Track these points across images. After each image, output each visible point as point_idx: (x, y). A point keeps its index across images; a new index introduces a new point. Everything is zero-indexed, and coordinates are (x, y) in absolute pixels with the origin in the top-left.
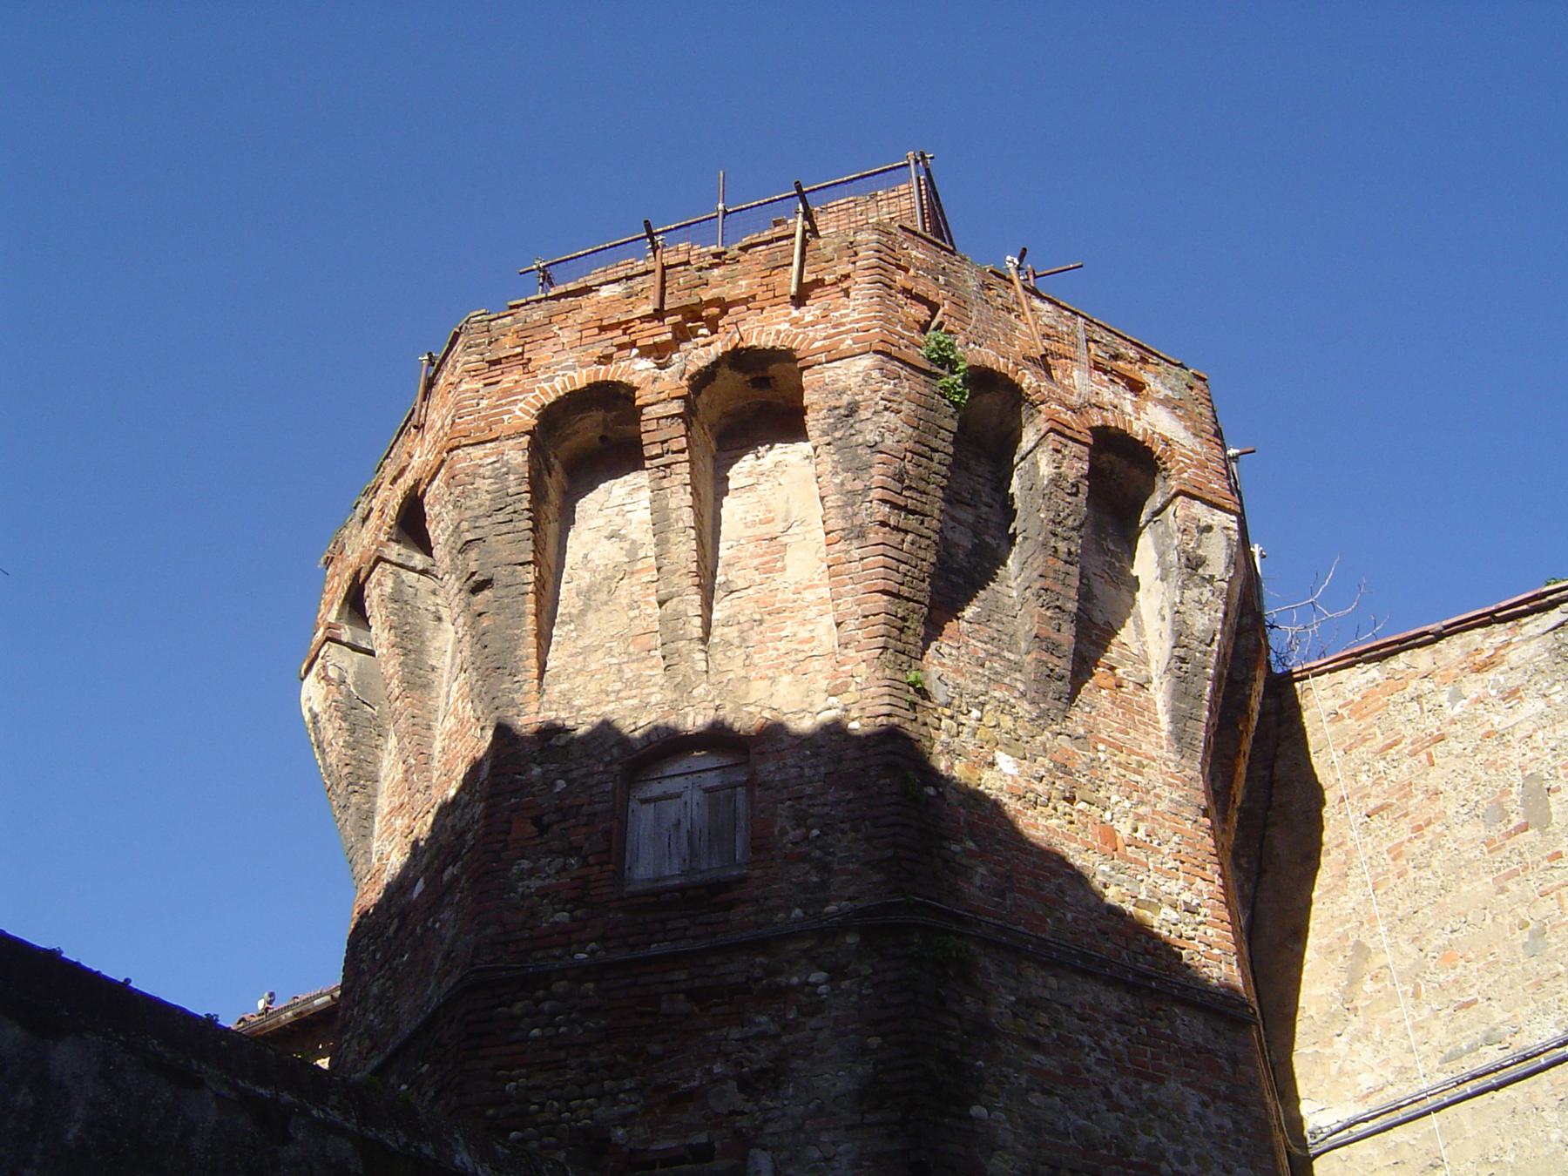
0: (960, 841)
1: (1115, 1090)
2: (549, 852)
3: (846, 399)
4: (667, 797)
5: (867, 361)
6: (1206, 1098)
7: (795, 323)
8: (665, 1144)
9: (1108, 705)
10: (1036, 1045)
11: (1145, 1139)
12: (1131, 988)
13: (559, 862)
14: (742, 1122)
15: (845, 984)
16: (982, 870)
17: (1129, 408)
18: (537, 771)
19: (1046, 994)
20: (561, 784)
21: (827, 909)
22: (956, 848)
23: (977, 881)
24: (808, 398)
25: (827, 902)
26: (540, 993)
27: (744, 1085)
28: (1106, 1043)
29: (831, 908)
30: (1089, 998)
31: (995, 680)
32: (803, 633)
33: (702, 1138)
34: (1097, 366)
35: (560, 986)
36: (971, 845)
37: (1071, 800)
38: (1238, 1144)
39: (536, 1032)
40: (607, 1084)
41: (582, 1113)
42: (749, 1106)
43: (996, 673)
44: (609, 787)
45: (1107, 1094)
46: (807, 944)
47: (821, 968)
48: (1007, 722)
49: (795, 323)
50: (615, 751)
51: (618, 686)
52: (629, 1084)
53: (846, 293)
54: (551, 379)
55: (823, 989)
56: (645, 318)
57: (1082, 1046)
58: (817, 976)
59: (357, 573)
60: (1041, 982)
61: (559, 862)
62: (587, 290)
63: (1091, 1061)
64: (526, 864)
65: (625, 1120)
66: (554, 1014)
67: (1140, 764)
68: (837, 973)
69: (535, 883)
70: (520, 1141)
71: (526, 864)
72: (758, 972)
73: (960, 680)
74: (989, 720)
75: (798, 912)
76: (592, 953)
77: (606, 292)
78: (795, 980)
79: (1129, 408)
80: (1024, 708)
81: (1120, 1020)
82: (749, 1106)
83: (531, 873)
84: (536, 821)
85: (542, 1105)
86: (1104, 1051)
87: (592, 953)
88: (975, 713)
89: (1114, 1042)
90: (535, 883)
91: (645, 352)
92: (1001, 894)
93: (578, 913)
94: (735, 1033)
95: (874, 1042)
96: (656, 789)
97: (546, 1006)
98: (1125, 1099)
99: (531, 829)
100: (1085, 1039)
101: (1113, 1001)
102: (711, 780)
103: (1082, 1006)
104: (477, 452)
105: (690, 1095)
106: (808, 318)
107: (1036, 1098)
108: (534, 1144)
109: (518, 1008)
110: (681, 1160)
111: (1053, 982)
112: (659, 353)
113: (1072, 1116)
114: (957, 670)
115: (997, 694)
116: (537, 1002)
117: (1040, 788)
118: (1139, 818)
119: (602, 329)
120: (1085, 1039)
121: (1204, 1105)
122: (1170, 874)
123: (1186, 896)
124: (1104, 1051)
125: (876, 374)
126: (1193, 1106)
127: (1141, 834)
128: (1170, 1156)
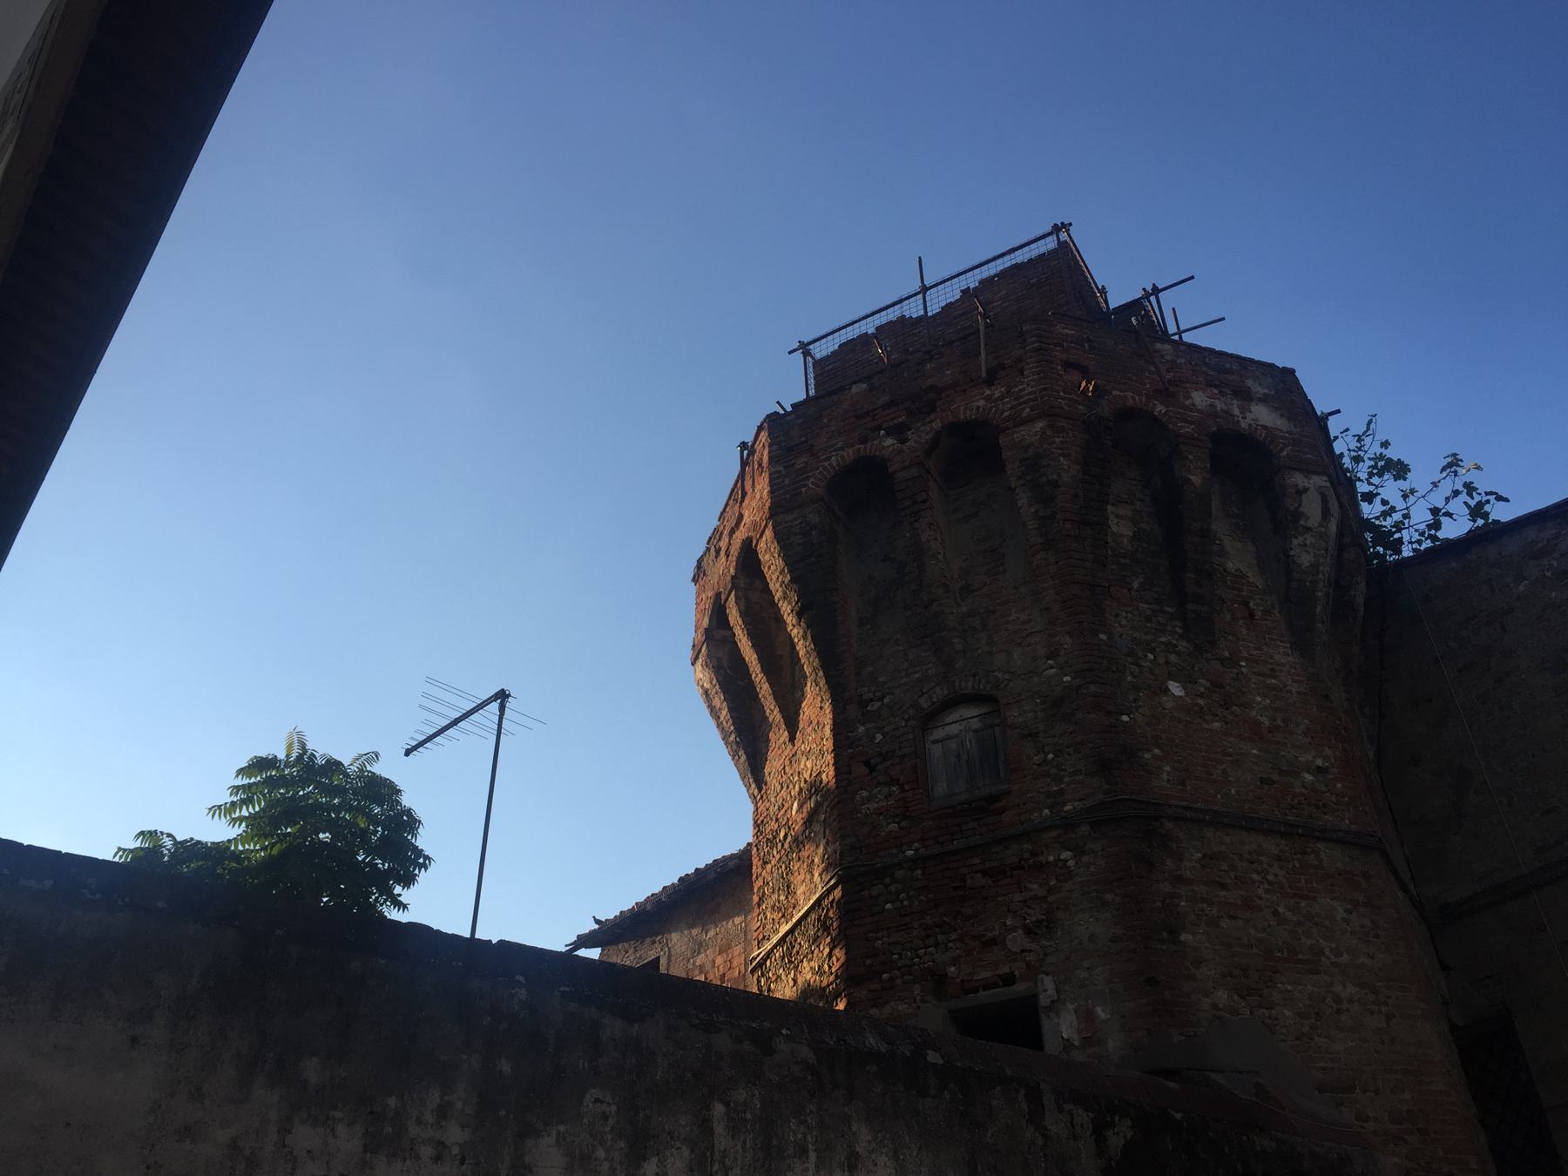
0: (1149, 750)
1: (1281, 910)
2: (879, 784)
3: (1031, 452)
4: (949, 738)
5: (1040, 425)
7: (988, 399)
8: (984, 974)
9: (1244, 631)
10: (1223, 886)
12: (1283, 835)
13: (886, 791)
14: (1031, 957)
15: (1085, 858)
16: (1167, 768)
17: (1237, 412)
18: (861, 729)
19: (1223, 848)
20: (879, 737)
21: (1068, 807)
22: (1147, 756)
23: (1165, 776)
24: (1006, 454)
25: (1065, 804)
26: (887, 880)
27: (1029, 932)
28: (1270, 877)
29: (1068, 807)
32: (1024, 617)
33: (1006, 970)
34: (1210, 384)
35: (899, 874)
36: (1157, 751)
38: (1377, 936)
39: (889, 906)
40: (940, 938)
41: (926, 958)
42: (1034, 946)
44: (911, 736)
45: (1276, 913)
46: (1055, 833)
47: (1067, 849)
48: (1173, 658)
49: (988, 399)
50: (911, 711)
51: (906, 665)
52: (954, 936)
53: (1021, 372)
54: (829, 459)
55: (1071, 863)
56: (885, 407)
57: (1253, 882)
58: (1066, 855)
59: (718, 595)
61: (886, 791)
62: (842, 389)
63: (1260, 891)
64: (865, 794)
65: (955, 961)
66: (898, 893)
67: (1273, 670)
68: (1079, 851)
69: (873, 806)
70: (891, 979)
71: (865, 794)
72: (1026, 855)
73: (1136, 635)
74: (1161, 660)
75: (1047, 811)
76: (917, 850)
77: (855, 389)
78: (1051, 858)
79: (1237, 412)
80: (1183, 645)
82: (1034, 946)
83: (869, 800)
84: (867, 763)
85: (900, 955)
86: (1270, 883)
87: (917, 850)
88: (1151, 656)
89: (1276, 875)
90: (873, 806)
91: (888, 434)
92: (1183, 784)
93: (904, 824)
94: (1017, 897)
95: (1109, 897)
96: (938, 734)
97: (893, 888)
98: (1289, 914)
99: (863, 770)
100: (1255, 877)
102: (976, 724)
103: (1250, 853)
104: (789, 518)
105: (993, 942)
106: (997, 394)
107: (1225, 923)
108: (899, 981)
109: (875, 891)
110: (996, 986)
112: (899, 431)
113: (1252, 931)
115: (1163, 639)
116: (886, 886)
117: (1201, 702)
119: (858, 417)
120: (1255, 877)
121: (1349, 912)
123: (1319, 762)
124: (1270, 883)
125: (1049, 432)
126: (1340, 914)
128: (1327, 951)
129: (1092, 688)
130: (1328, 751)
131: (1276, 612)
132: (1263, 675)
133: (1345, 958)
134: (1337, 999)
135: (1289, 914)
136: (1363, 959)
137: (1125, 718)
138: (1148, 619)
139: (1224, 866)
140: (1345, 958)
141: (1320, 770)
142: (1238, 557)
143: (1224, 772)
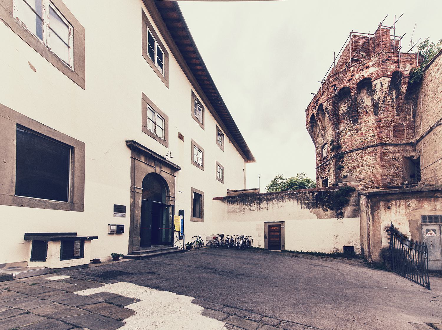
6: (371, 156)
10: (349, 160)
11: (361, 163)
30: (356, 153)
31: (349, 124)
36: (343, 145)
37: (358, 132)
43: (348, 123)
60: (350, 154)
73: (344, 127)
81: (360, 153)
92: (347, 148)
100: (355, 157)
101: (359, 152)
111: (352, 153)
114: (344, 126)
115: (349, 126)
117: (353, 134)
118: (367, 129)
122: (371, 133)
123: (373, 134)
127: (367, 131)
129: (335, 139)
130: (376, 132)
131: (373, 109)
132: (366, 123)
133: (368, 163)
134: (364, 169)
135: (360, 161)
136: (371, 163)
137: (339, 142)
138: (347, 123)
139: (350, 157)
140: (368, 163)
141: (373, 136)
142: (368, 102)
143: (354, 143)
